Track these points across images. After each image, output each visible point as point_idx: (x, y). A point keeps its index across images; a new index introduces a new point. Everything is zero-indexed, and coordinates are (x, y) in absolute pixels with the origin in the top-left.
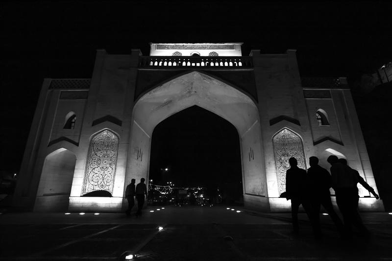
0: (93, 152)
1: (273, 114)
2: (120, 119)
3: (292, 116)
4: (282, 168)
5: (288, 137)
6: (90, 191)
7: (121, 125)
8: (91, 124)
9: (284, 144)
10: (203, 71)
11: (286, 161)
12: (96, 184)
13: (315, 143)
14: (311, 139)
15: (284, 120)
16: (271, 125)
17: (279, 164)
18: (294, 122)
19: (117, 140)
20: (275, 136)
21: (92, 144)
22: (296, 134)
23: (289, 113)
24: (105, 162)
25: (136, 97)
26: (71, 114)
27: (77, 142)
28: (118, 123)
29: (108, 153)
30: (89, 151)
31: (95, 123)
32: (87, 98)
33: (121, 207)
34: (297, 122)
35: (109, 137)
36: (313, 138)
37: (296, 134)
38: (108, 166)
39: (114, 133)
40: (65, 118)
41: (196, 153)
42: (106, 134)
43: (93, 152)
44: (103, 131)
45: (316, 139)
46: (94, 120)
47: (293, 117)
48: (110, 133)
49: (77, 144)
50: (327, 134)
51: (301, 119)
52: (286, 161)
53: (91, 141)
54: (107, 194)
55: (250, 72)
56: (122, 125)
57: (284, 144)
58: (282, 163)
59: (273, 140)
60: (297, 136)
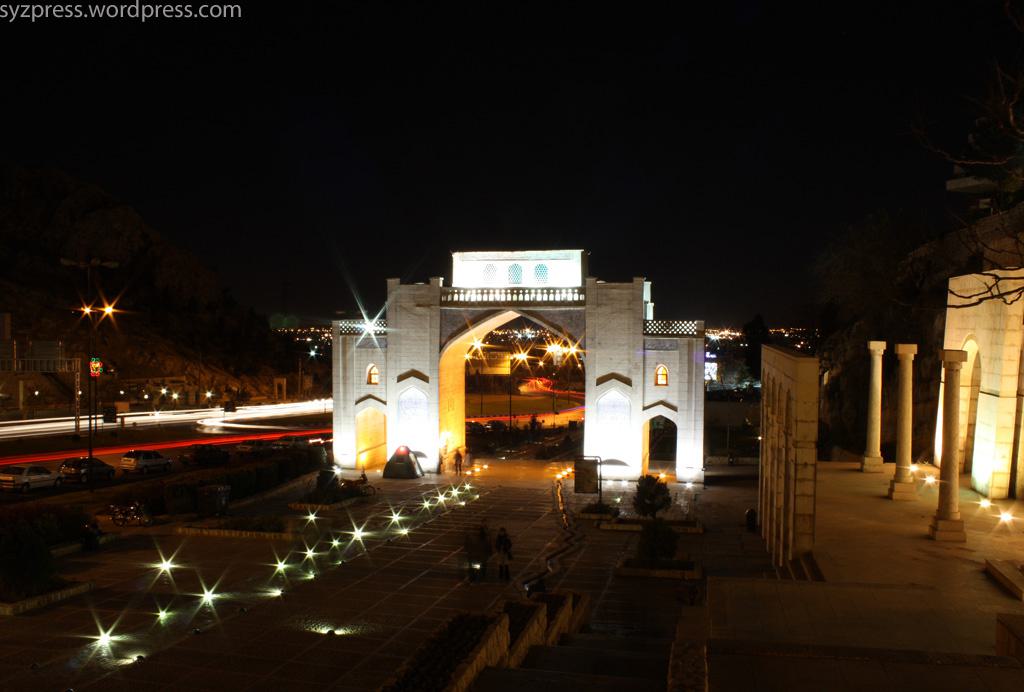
2: (427, 374)
13: (645, 408)
15: (613, 380)
21: (399, 403)
23: (623, 373)
25: (442, 347)
26: (371, 365)
27: (384, 400)
28: (425, 379)
31: (401, 378)
32: (386, 346)
34: (628, 382)
41: (520, 413)
42: (413, 387)
45: (646, 405)
46: (398, 374)
49: (385, 403)
51: (636, 379)
55: (578, 311)
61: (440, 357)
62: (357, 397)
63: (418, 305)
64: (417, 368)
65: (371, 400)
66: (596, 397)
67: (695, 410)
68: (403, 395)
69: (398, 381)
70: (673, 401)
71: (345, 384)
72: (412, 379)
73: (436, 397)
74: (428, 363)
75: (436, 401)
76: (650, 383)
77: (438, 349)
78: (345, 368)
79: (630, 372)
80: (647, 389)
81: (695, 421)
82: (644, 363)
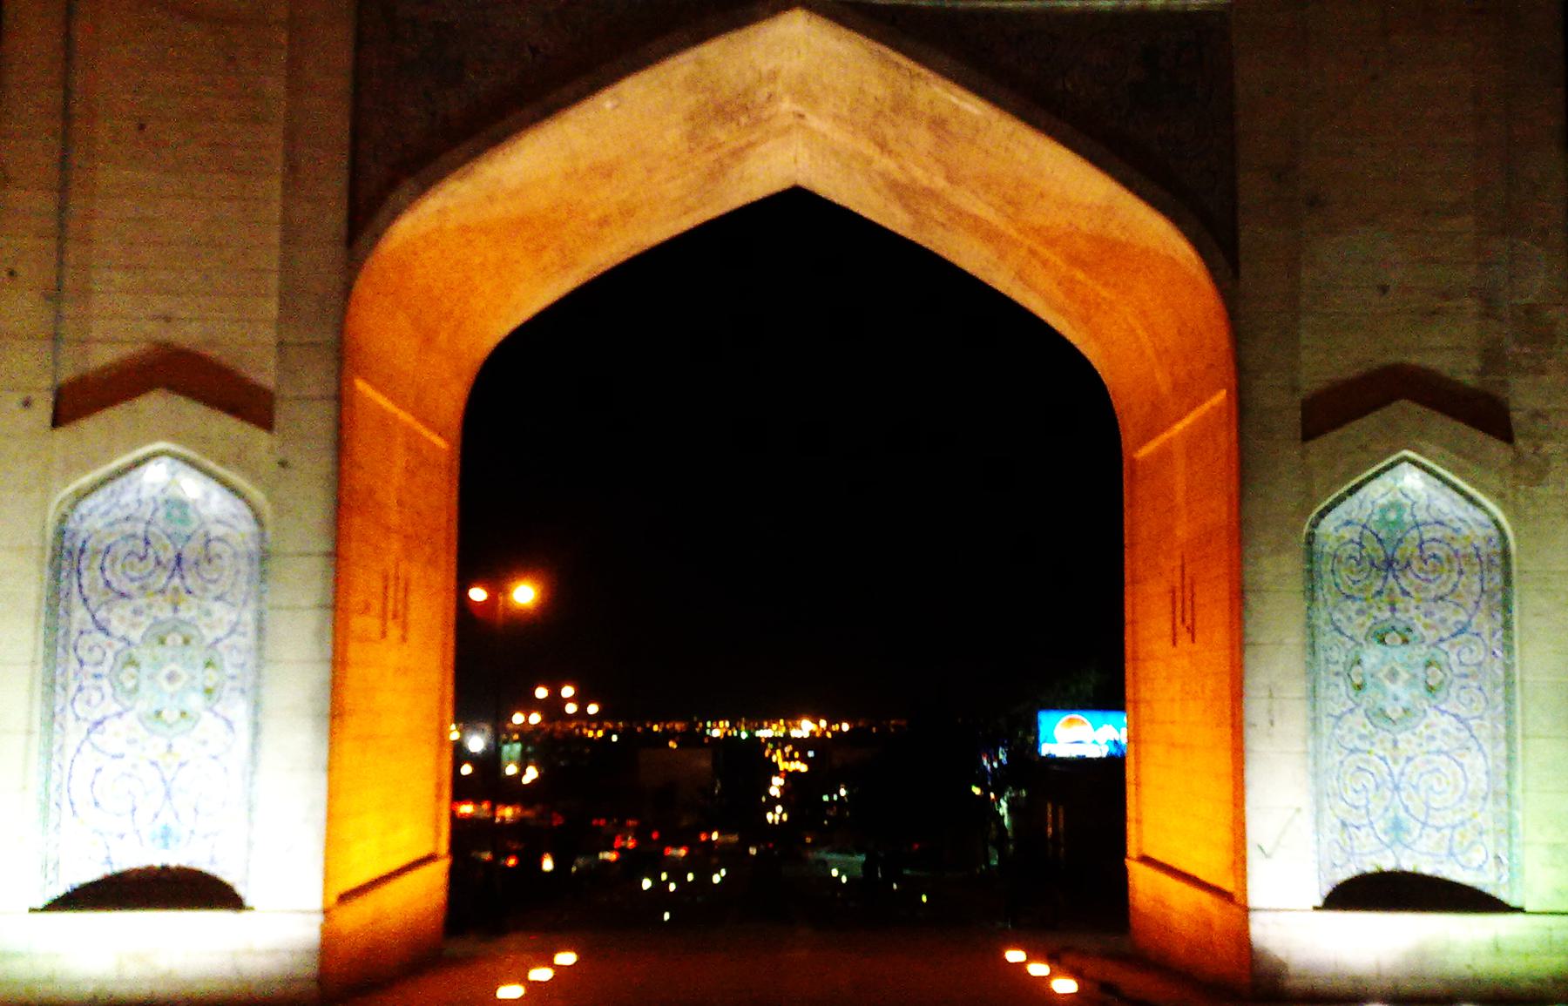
1: (1324, 360)
2: (264, 373)
3: (1463, 369)
4: (1357, 721)
5: (1421, 516)
6: (93, 872)
7: (265, 421)
8: (44, 409)
9: (1389, 563)
11: (1393, 675)
15: (1404, 403)
16: (1308, 436)
17: (1337, 696)
19: (246, 527)
20: (1328, 509)
22: (1471, 499)
23: (1448, 353)
24: (171, 677)
28: (248, 403)
29: (184, 614)
33: (310, 968)
35: (183, 505)
37: (1471, 499)
38: (195, 701)
39: (224, 483)
43: (80, 614)
44: (137, 464)
46: (67, 373)
47: (1468, 380)
48: (192, 487)
53: (61, 533)
54: (196, 890)
56: (280, 420)
57: (1389, 563)
58: (1360, 687)
59: (1311, 539)
60: (1480, 515)
64: (188, 334)
66: (1310, 498)
68: (85, 506)
69: (60, 418)
73: (313, 507)
74: (272, 307)
75: (324, 545)
77: (335, 219)
79: (1493, 358)
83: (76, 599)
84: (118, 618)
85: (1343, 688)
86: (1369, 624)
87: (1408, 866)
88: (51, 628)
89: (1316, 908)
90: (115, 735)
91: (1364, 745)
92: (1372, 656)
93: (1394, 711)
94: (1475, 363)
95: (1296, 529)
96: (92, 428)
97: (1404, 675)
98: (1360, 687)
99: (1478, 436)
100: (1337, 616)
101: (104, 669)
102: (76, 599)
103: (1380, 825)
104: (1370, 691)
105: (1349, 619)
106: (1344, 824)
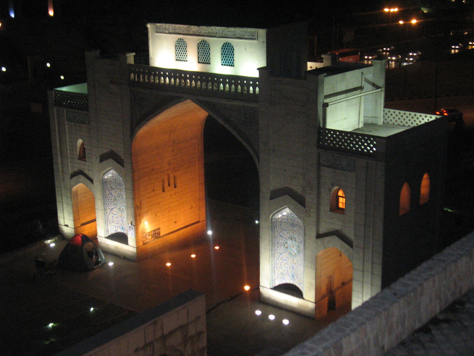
0: (107, 192)
3: (299, 190)
9: (293, 224)
10: (198, 100)
12: (117, 225)
13: (319, 236)
14: (314, 229)
16: (271, 199)
18: (299, 201)
23: (296, 187)
25: (133, 131)
26: (80, 141)
30: (104, 191)
36: (318, 226)
40: (76, 147)
43: (107, 192)
45: (322, 231)
46: (101, 153)
50: (337, 226)
51: (310, 199)
52: (293, 246)
58: (287, 248)
59: (272, 219)
61: (132, 141)
62: (70, 172)
63: (112, 82)
65: (82, 178)
67: (373, 251)
69: (101, 161)
70: (350, 234)
71: (62, 156)
72: (110, 160)
76: (325, 208)
78: (60, 141)
80: (322, 213)
81: (372, 263)
82: (319, 183)
83: (107, 189)
84: (113, 192)
85: (283, 248)
86: (289, 235)
87: (295, 284)
88: (103, 195)
89: (271, 289)
90: (115, 211)
91: (288, 259)
92: (290, 242)
93: (293, 254)
94: (301, 189)
95: (269, 217)
96: (104, 163)
97: (295, 247)
98: (287, 248)
99: (300, 206)
100: (281, 234)
101: (112, 201)
102: (107, 189)
103: (290, 275)
104: (289, 249)
105: (285, 234)
106: (282, 273)
